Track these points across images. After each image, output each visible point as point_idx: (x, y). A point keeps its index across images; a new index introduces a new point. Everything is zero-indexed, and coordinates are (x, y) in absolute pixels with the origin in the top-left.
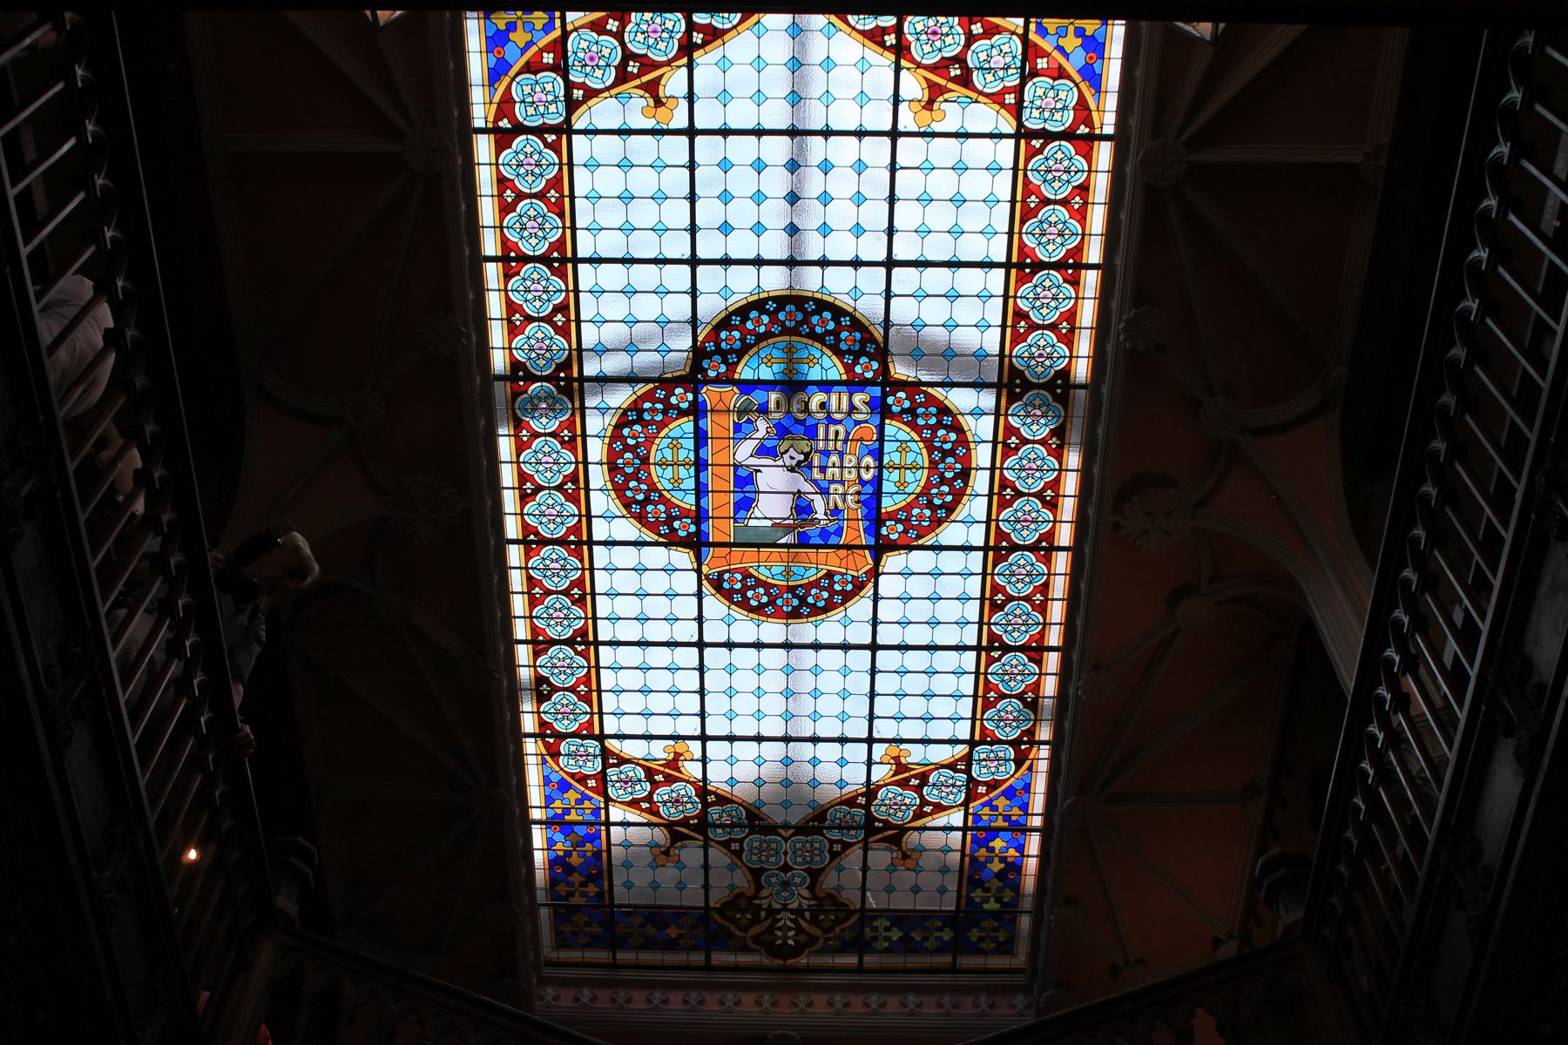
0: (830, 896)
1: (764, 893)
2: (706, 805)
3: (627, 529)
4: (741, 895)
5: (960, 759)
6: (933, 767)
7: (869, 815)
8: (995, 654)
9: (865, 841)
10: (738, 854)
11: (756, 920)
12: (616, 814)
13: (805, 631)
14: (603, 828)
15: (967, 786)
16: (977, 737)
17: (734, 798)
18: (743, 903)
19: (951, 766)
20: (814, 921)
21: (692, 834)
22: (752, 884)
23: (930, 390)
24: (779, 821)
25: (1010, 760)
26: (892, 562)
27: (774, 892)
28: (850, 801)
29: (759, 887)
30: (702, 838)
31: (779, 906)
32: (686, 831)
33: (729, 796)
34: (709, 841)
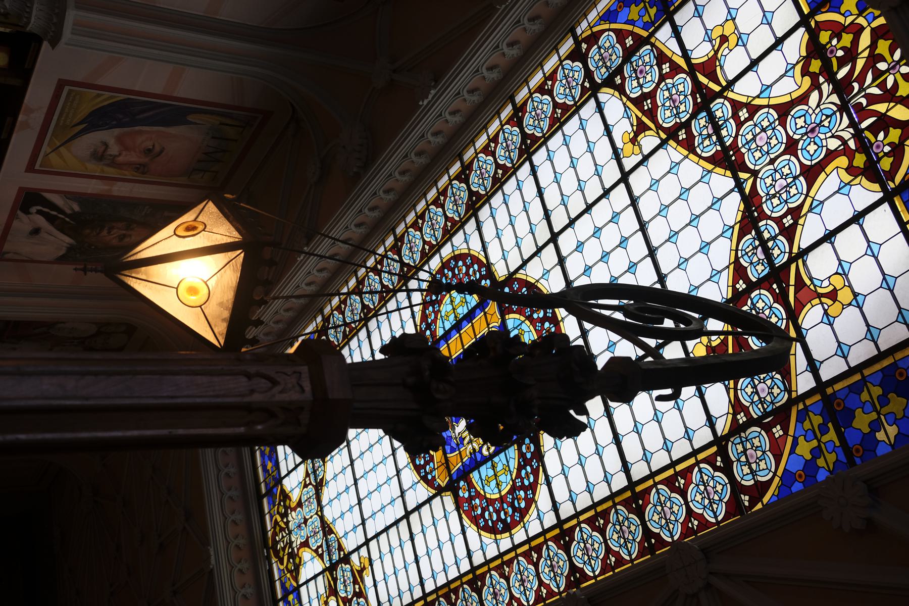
0: (805, 72)
1: (834, 144)
2: (752, 286)
3: (542, 497)
4: (850, 170)
6: (629, 104)
9: (720, 95)
11: (884, 123)
12: (804, 383)
14: (829, 391)
17: (732, 260)
18: (860, 160)
20: (851, 55)
21: (792, 281)
22: (828, 170)
23: (418, 323)
24: (736, 197)
27: (829, 134)
28: (689, 145)
29: (831, 155)
30: (793, 267)
32: (792, 290)
33: (732, 267)
34: (793, 255)
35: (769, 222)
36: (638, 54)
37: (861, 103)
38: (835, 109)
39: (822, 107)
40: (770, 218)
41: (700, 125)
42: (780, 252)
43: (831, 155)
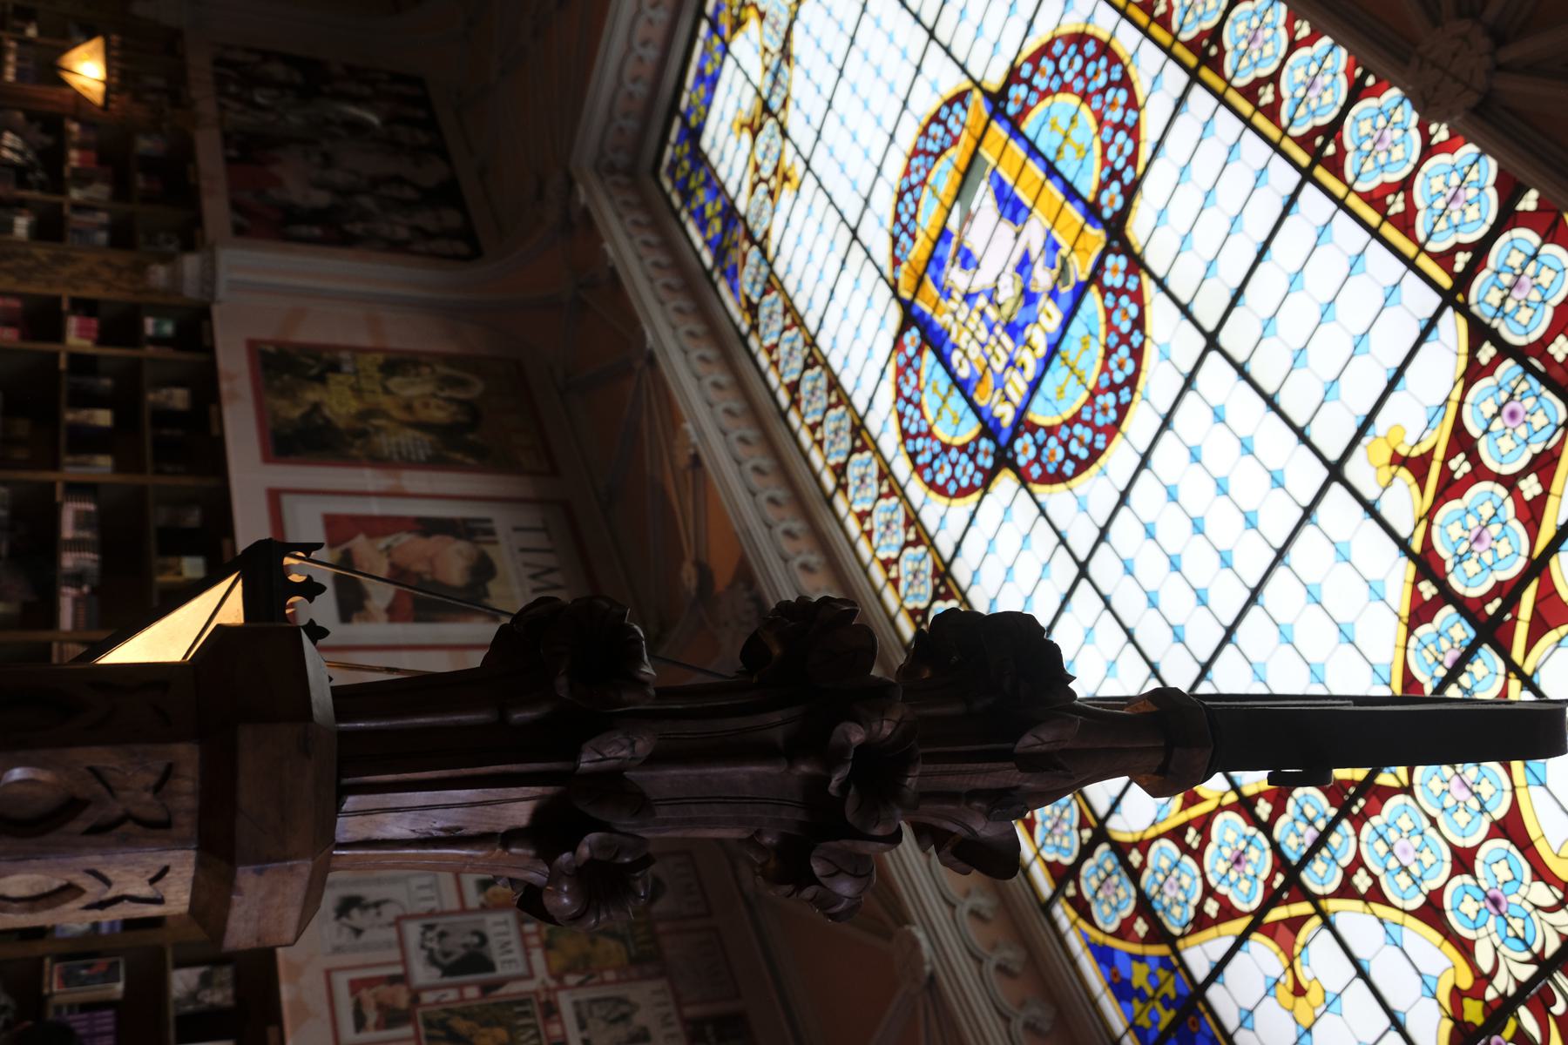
4: (1457, 994)
5: (1474, 347)
6: (1452, 408)
7: (1468, 609)
8: (1331, 150)
10: (1376, 895)
13: (1140, 424)
15: (1529, 369)
16: (1446, 282)
19: (1473, 373)
25: (1537, 250)
26: (1137, 229)
27: (1497, 942)
28: (1420, 613)
29: (1466, 948)
31: (1533, 969)
34: (1323, 903)
35: (1353, 840)
36: (1543, 389)
37: (1554, 1002)
38: (1536, 948)
39: (1534, 915)
40: (1358, 841)
41: (1451, 628)
42: (1321, 877)
43: (1466, 948)
